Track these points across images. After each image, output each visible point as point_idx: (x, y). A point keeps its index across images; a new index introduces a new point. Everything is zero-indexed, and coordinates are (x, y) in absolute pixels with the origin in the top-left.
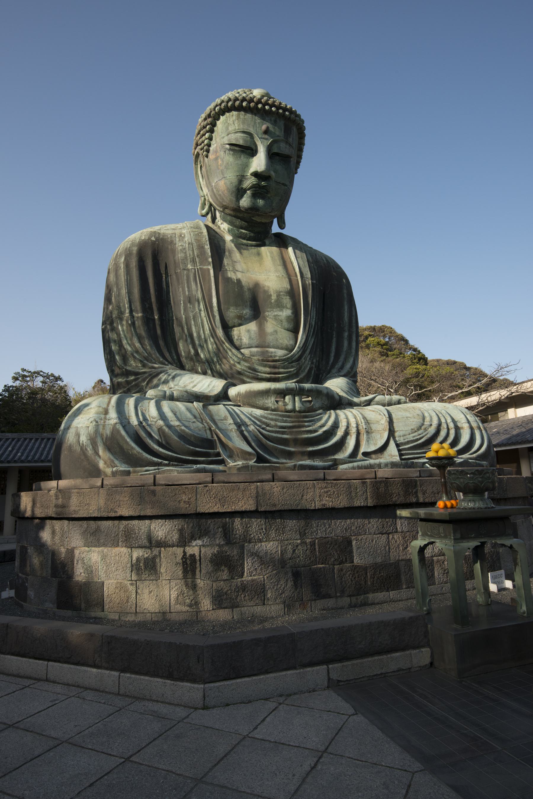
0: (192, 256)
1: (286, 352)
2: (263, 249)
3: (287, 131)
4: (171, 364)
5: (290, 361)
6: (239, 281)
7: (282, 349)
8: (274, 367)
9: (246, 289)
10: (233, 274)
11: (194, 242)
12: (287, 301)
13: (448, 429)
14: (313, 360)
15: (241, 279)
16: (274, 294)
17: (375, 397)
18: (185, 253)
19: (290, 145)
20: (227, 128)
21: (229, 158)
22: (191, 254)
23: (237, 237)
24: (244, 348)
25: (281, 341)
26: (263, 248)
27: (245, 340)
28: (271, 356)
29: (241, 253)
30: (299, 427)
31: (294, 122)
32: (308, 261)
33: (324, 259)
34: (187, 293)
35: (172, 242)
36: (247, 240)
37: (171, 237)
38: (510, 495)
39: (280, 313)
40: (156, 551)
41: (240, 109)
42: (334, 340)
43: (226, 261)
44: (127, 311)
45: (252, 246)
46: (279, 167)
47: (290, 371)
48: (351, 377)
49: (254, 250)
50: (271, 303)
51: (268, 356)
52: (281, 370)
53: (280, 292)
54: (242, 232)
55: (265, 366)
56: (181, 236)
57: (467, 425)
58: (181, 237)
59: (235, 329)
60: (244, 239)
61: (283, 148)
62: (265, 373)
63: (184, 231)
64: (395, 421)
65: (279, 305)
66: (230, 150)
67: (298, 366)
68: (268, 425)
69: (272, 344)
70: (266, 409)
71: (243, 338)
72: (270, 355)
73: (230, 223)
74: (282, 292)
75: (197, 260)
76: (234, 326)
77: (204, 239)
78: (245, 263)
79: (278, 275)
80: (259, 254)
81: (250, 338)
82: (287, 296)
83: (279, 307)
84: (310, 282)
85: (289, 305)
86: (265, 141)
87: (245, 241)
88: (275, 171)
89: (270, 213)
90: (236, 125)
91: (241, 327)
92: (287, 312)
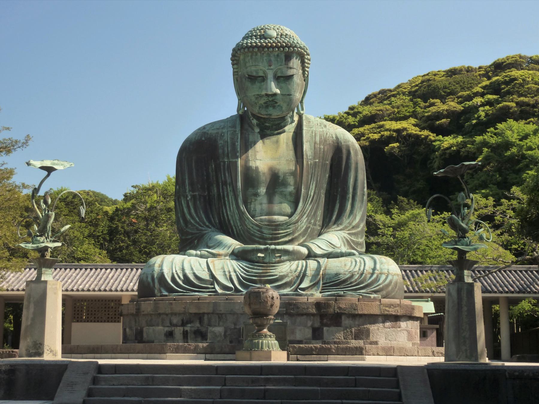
0: (226, 152)
1: (287, 218)
4: (214, 226)
6: (257, 168)
7: (284, 215)
9: (261, 174)
10: (254, 163)
12: (291, 180)
14: (311, 220)
18: (223, 149)
20: (245, 65)
26: (282, 135)
28: (275, 222)
32: (315, 143)
34: (223, 179)
35: (216, 141)
38: (360, 312)
39: (284, 189)
40: (173, 328)
44: (187, 191)
47: (287, 232)
48: (349, 230)
55: (269, 229)
58: (222, 136)
60: (268, 129)
63: (224, 131)
66: (249, 78)
71: (257, 209)
80: (277, 142)
84: (312, 162)
86: (271, 71)
87: (268, 132)
92: (291, 189)
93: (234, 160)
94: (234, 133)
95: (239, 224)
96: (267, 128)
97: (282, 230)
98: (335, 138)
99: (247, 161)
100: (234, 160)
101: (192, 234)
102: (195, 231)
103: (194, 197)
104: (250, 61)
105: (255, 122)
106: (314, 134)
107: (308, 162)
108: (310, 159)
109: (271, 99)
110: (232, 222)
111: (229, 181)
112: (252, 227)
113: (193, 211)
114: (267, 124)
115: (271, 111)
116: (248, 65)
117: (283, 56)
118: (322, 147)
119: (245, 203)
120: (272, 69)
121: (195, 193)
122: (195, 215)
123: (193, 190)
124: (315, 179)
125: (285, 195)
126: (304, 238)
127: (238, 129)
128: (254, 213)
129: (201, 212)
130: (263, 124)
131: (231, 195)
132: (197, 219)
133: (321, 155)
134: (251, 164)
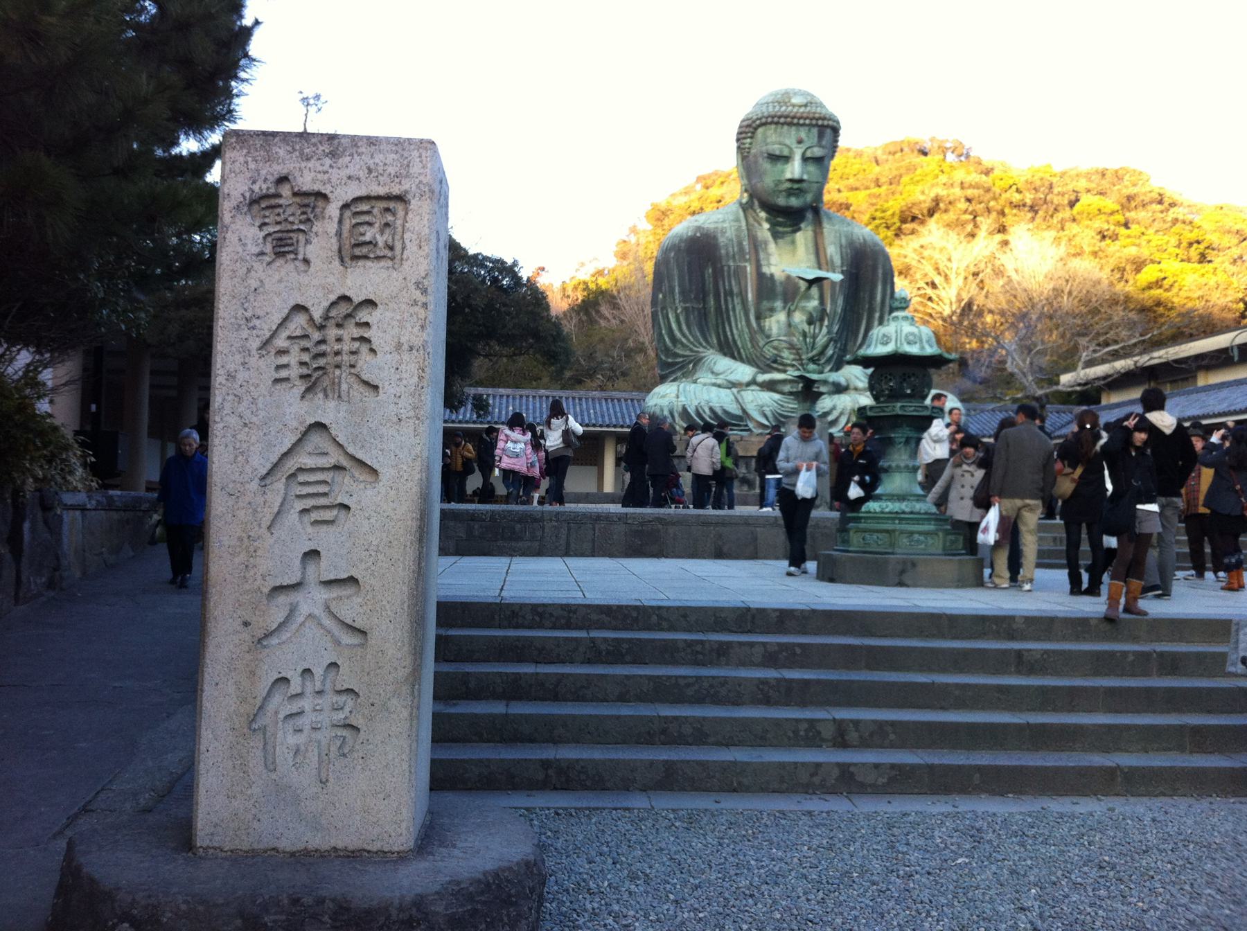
2: (799, 235)
3: (821, 136)
4: (712, 347)
6: (772, 275)
19: (823, 147)
21: (766, 165)
23: (774, 225)
27: (775, 331)
31: (828, 126)
32: (841, 246)
35: (715, 238)
41: (777, 123)
42: (864, 322)
43: (762, 255)
46: (812, 168)
49: (788, 239)
58: (723, 232)
61: (817, 152)
73: (767, 212)
80: (793, 242)
81: (779, 328)
87: (781, 229)
88: (808, 173)
94: (739, 229)
99: (758, 266)
101: (683, 356)
102: (688, 353)
103: (686, 309)
105: (763, 215)
109: (796, 186)
110: (739, 343)
111: (735, 290)
113: (684, 327)
116: (769, 140)
117: (815, 131)
119: (759, 317)
123: (684, 300)
127: (744, 224)
131: (738, 308)
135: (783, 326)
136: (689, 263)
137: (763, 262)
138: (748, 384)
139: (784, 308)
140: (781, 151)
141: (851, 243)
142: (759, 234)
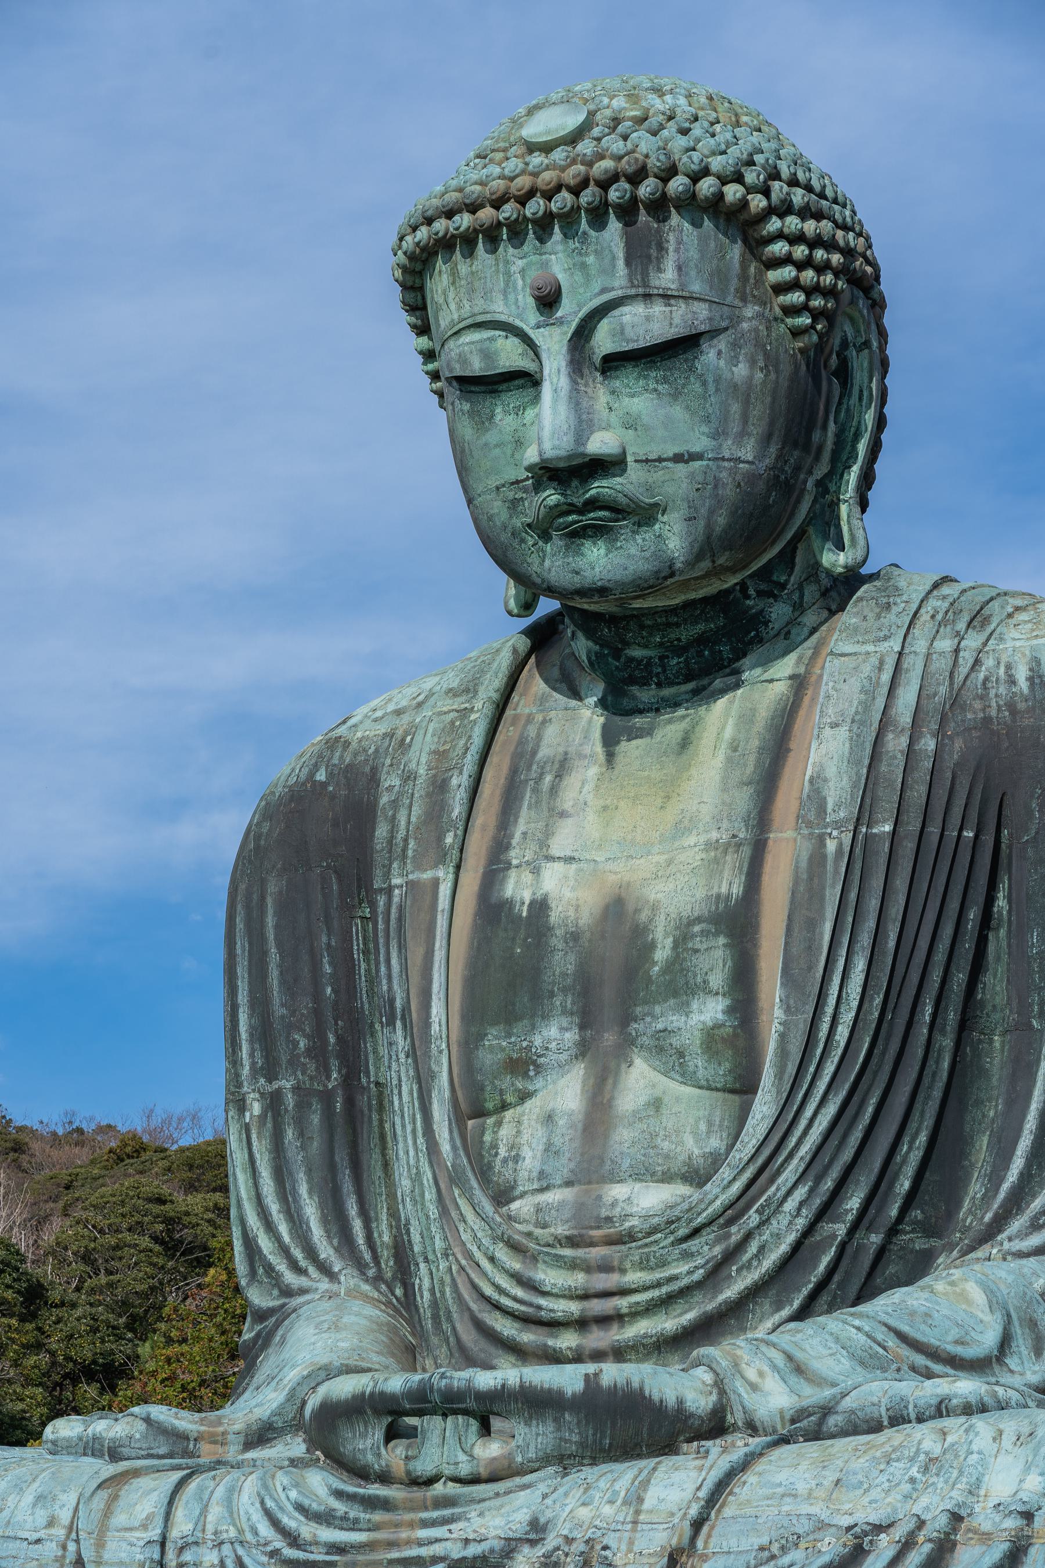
0: (401, 834)
1: (682, 1189)
4: (360, 1266)
5: (682, 1232)
6: (540, 906)
7: (667, 1178)
8: (606, 1268)
9: (556, 942)
10: (527, 877)
11: (422, 771)
12: (714, 962)
13: (907, 1545)
15: (551, 896)
16: (666, 935)
17: (844, 1395)
18: (393, 821)
19: (667, 297)
22: (403, 823)
24: (522, 1196)
25: (666, 1145)
26: (721, 703)
27: (531, 1161)
28: (609, 1219)
29: (610, 756)
30: (391, 1544)
33: (1022, 674)
35: (374, 779)
36: (659, 685)
37: (377, 751)
39: (675, 1020)
43: (524, 823)
45: (676, 705)
50: (649, 980)
51: (598, 1218)
52: (634, 1277)
53: (691, 923)
54: (632, 659)
55: (573, 1265)
56: (403, 740)
57: (1012, 1523)
59: (509, 1114)
60: (644, 683)
62: (571, 1298)
64: (728, 1512)
65: (680, 986)
67: (718, 1250)
68: (293, 1539)
69: (626, 1163)
70: (362, 1473)
71: (527, 1153)
72: (604, 1213)
74: (699, 920)
75: (412, 844)
76: (504, 1106)
77: (462, 742)
78: (605, 808)
79: (714, 835)
80: (685, 743)
82: (716, 934)
83: (675, 994)
85: (717, 979)
86: (556, 331)
87: (645, 695)
88: (631, 423)
89: (672, 575)
90: (453, 306)
91: (529, 1104)
92: (711, 1011)
93: (427, 875)
95: (439, 1244)
96: (641, 674)
97: (643, 1265)
98: (1023, 685)
100: (427, 875)
104: (451, 295)
106: (886, 677)
107: (821, 840)
108: (838, 825)
112: (492, 1259)
114: (637, 653)
115: (599, 561)
118: (928, 744)
120: (561, 322)
121: (276, 1085)
122: (274, 1207)
124: (865, 939)
125: (681, 1054)
126: (786, 1312)
128: (508, 1174)
129: (303, 1189)
130: (617, 654)
132: (283, 1229)
133: (918, 793)
134: (509, 889)
135: (565, 1135)
136: (284, 909)
137: (514, 855)
138: (261, 1435)
139: (583, 1049)
140: (487, 356)
141: (947, 710)
142: (551, 733)
